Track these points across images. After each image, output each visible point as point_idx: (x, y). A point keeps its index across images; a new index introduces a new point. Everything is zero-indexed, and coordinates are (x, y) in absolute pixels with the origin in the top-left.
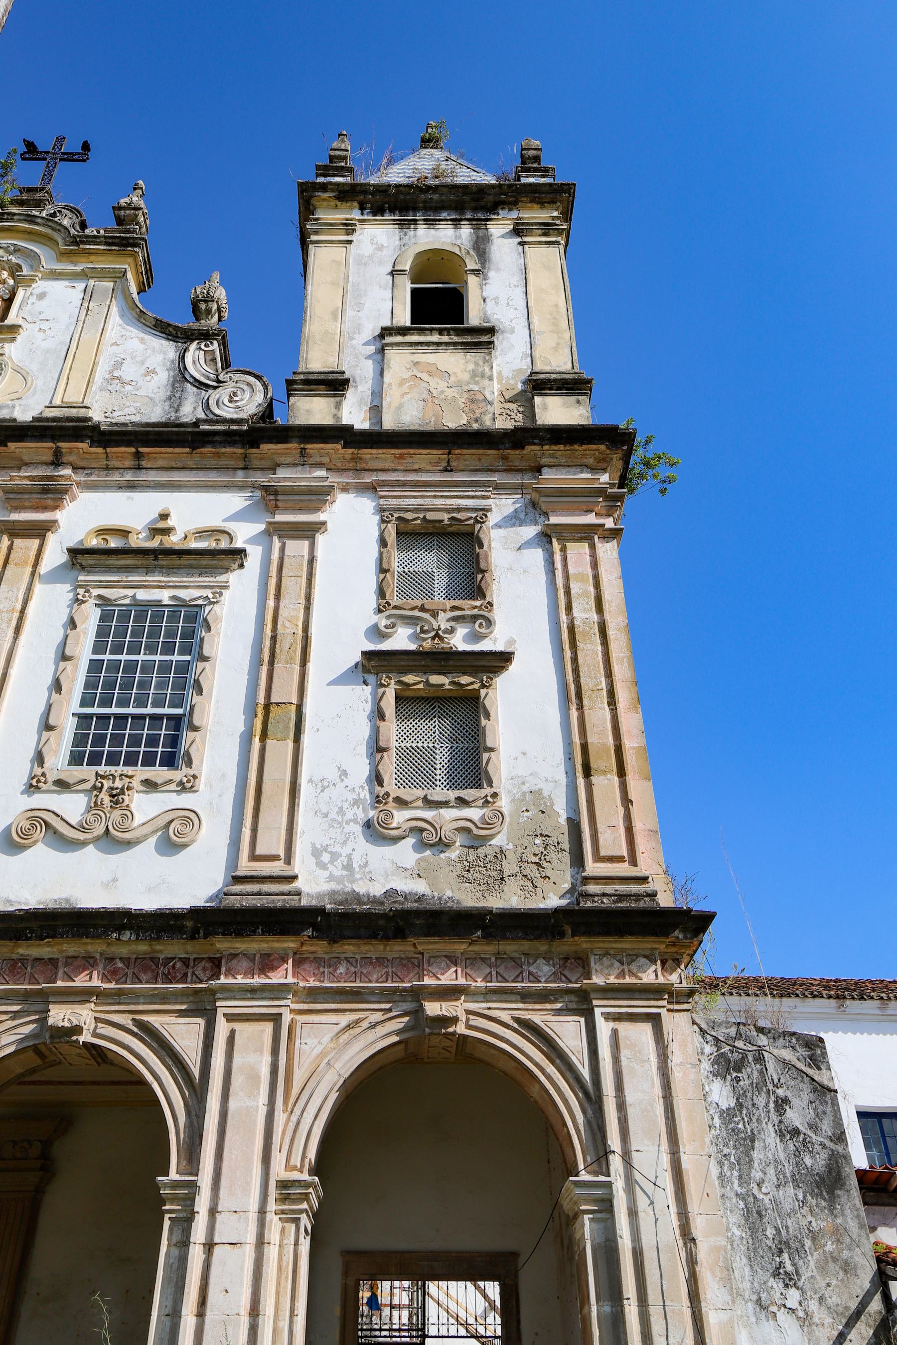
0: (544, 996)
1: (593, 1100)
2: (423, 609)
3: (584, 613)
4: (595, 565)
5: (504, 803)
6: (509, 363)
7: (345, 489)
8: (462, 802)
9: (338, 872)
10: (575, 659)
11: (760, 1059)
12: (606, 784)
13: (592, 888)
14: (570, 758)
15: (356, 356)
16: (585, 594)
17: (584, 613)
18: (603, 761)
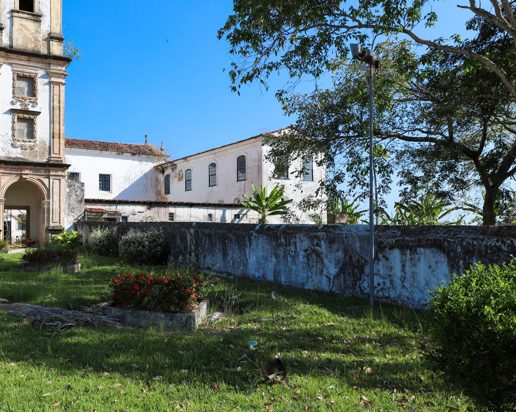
0: (42, 175)
1: (48, 190)
2: (23, 98)
3: (56, 104)
4: (59, 92)
5: (38, 142)
6: (45, 27)
7: (4, 63)
8: (30, 142)
9: (7, 153)
10: (53, 114)
11: (74, 185)
12: (56, 140)
13: (52, 159)
14: (50, 134)
15: (5, 18)
16: (57, 99)
17: (56, 104)
18: (56, 136)
